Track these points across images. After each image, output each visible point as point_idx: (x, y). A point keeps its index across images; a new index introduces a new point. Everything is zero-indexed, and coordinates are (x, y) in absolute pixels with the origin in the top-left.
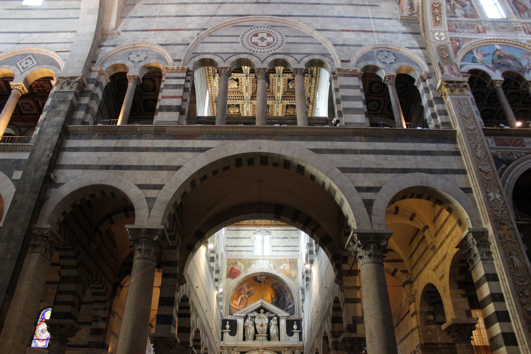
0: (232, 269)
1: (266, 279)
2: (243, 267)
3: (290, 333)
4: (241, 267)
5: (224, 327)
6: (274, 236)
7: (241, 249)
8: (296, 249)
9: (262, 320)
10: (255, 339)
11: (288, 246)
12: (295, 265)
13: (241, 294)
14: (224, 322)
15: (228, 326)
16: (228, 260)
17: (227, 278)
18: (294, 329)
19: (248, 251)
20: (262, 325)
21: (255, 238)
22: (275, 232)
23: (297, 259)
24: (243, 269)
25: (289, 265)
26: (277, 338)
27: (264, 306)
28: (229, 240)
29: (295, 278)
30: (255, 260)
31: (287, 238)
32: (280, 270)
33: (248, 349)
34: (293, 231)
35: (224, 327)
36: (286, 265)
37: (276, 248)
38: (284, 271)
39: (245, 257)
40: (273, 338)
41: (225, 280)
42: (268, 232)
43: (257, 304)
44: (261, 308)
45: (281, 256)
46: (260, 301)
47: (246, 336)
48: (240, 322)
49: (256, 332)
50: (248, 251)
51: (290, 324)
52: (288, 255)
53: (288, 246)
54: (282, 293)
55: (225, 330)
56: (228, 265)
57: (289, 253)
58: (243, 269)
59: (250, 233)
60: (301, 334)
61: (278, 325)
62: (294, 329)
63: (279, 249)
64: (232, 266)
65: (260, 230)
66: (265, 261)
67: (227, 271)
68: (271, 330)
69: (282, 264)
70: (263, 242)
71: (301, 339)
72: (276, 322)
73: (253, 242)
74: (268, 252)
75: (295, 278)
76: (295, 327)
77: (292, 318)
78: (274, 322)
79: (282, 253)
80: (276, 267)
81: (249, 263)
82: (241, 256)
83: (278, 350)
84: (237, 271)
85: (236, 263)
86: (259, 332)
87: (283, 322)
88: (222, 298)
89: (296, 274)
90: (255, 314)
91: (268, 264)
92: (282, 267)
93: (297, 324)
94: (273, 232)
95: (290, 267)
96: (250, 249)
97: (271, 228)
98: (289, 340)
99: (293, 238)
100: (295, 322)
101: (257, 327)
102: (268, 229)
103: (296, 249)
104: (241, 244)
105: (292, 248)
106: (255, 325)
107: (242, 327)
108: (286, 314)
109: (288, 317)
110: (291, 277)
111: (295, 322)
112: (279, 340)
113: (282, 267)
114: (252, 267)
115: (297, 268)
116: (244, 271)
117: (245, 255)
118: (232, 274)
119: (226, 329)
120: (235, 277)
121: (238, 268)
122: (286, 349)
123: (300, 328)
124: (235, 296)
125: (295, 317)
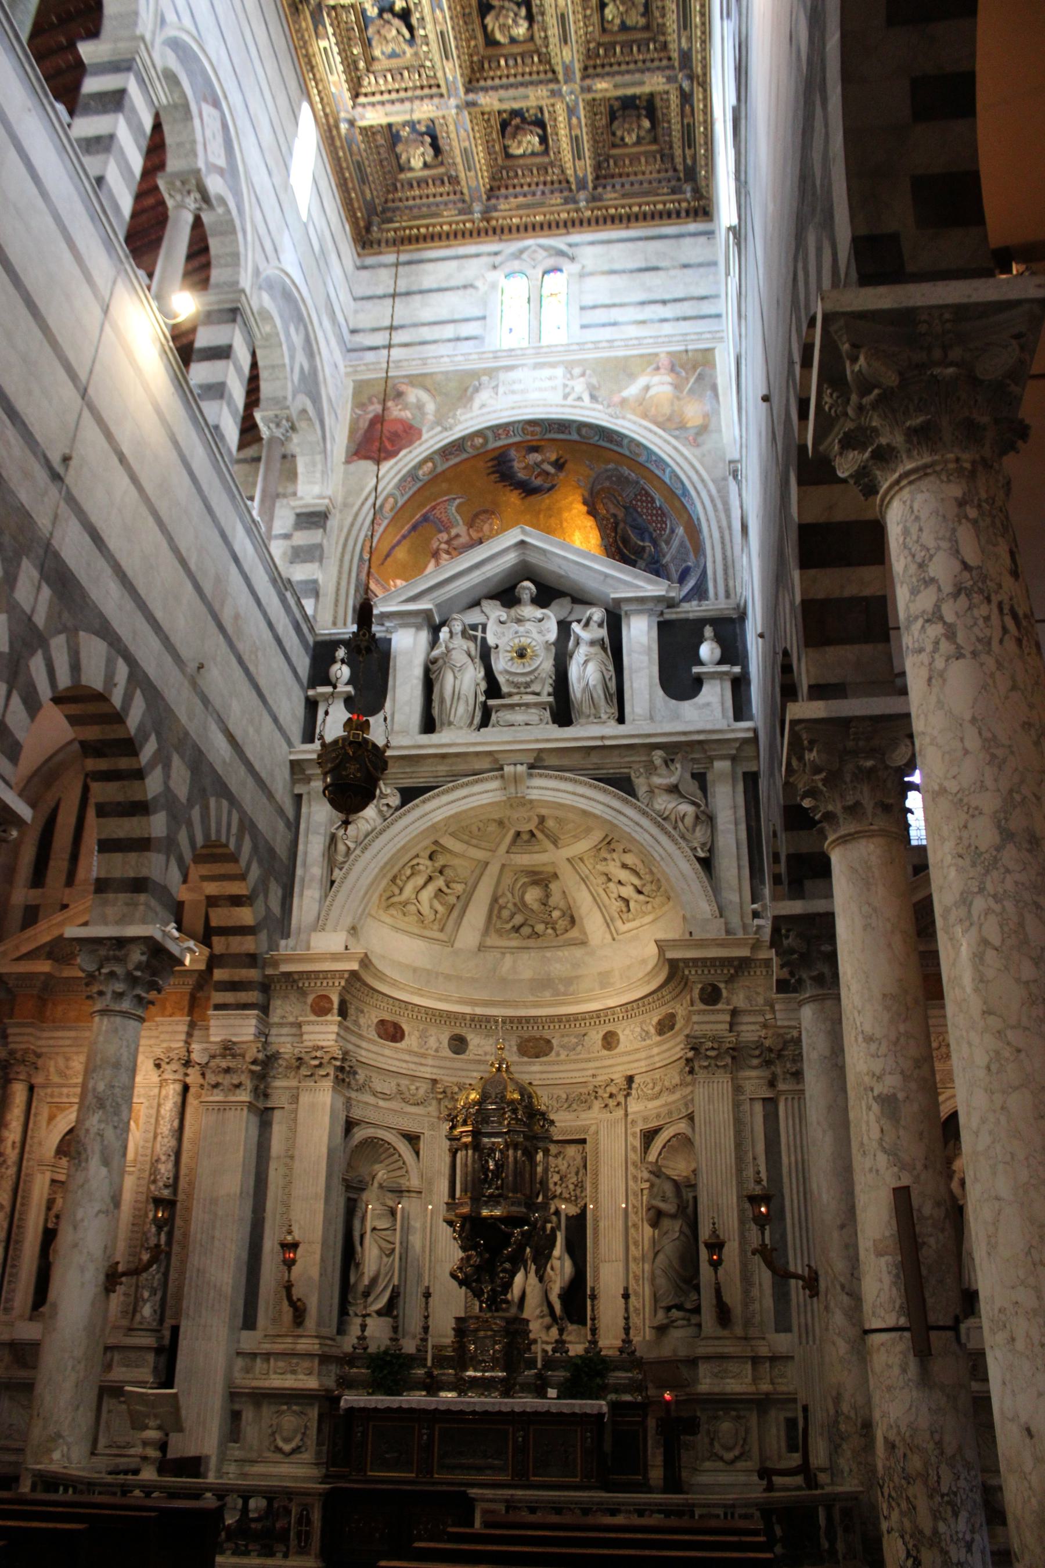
0: (378, 420)
1: (559, 465)
2: (430, 407)
3: (679, 679)
4: (420, 407)
5: (320, 675)
6: (588, 270)
7: (426, 333)
8: (706, 308)
9: (528, 631)
10: (485, 722)
11: (664, 302)
12: (700, 378)
13: (436, 555)
14: (322, 654)
15: (342, 672)
16: (360, 387)
17: (348, 461)
18: (701, 663)
19: (458, 339)
20: (522, 654)
21: (493, 286)
22: (599, 249)
23: (712, 350)
24: (430, 417)
25: (668, 379)
26: (607, 710)
27: (534, 559)
28: (368, 305)
29: (703, 429)
30: (491, 372)
31: (656, 269)
32: (624, 402)
33: (442, 768)
34: (688, 241)
35: (320, 675)
36: (656, 379)
37: (601, 316)
38: (643, 407)
39: (445, 365)
40: (586, 710)
41: (342, 467)
42: (561, 253)
43: (498, 551)
44: (525, 571)
45: (627, 343)
46: (513, 536)
47: (435, 712)
48: (408, 646)
49: (493, 689)
50: (458, 339)
51: (676, 644)
52: (671, 335)
53: (664, 302)
54: (642, 531)
55: (321, 689)
56: (359, 403)
57: (668, 329)
58: (430, 417)
59: (472, 269)
60: (739, 685)
61: (614, 648)
62: (701, 663)
63: (615, 314)
64: (376, 408)
65: (522, 251)
66: (547, 372)
67: (352, 432)
68: (574, 671)
69: (632, 377)
70: (536, 301)
71: (740, 709)
72: (603, 633)
73: (485, 303)
74: (560, 325)
75: (703, 429)
76: (707, 650)
77: (692, 609)
78: (587, 634)
79: (633, 331)
80: (602, 394)
81: (464, 387)
82: (424, 361)
83: (613, 765)
84: (399, 428)
85: (399, 395)
86: (505, 689)
87: (640, 633)
88: (320, 547)
89: (706, 416)
90: (494, 612)
91: (559, 382)
92: (632, 390)
93: (718, 639)
94: (589, 251)
95: (677, 387)
96: (466, 330)
97: (575, 238)
98: (677, 717)
99: (685, 266)
100: (708, 631)
101: (501, 664)
102: (559, 242)
103: (706, 308)
104: (427, 314)
105: (687, 309)
106: (485, 654)
107: (418, 672)
108: (652, 588)
109: (671, 603)
110: (682, 427)
111: (708, 631)
112: (621, 720)
113: (632, 390)
114: (477, 403)
115: (714, 388)
116: (438, 423)
117: (446, 358)
118: (376, 440)
119: (327, 681)
120: (391, 454)
121: (407, 415)
122: (658, 756)
123: (732, 651)
124: (401, 554)
125: (715, 604)
